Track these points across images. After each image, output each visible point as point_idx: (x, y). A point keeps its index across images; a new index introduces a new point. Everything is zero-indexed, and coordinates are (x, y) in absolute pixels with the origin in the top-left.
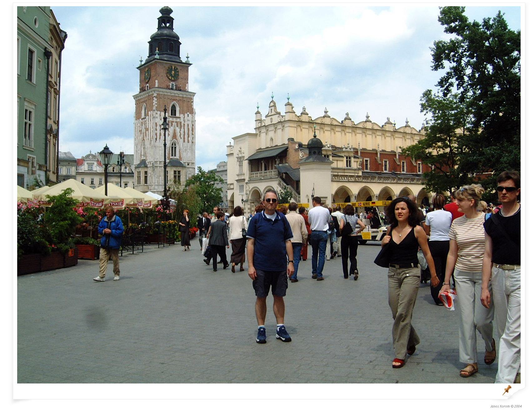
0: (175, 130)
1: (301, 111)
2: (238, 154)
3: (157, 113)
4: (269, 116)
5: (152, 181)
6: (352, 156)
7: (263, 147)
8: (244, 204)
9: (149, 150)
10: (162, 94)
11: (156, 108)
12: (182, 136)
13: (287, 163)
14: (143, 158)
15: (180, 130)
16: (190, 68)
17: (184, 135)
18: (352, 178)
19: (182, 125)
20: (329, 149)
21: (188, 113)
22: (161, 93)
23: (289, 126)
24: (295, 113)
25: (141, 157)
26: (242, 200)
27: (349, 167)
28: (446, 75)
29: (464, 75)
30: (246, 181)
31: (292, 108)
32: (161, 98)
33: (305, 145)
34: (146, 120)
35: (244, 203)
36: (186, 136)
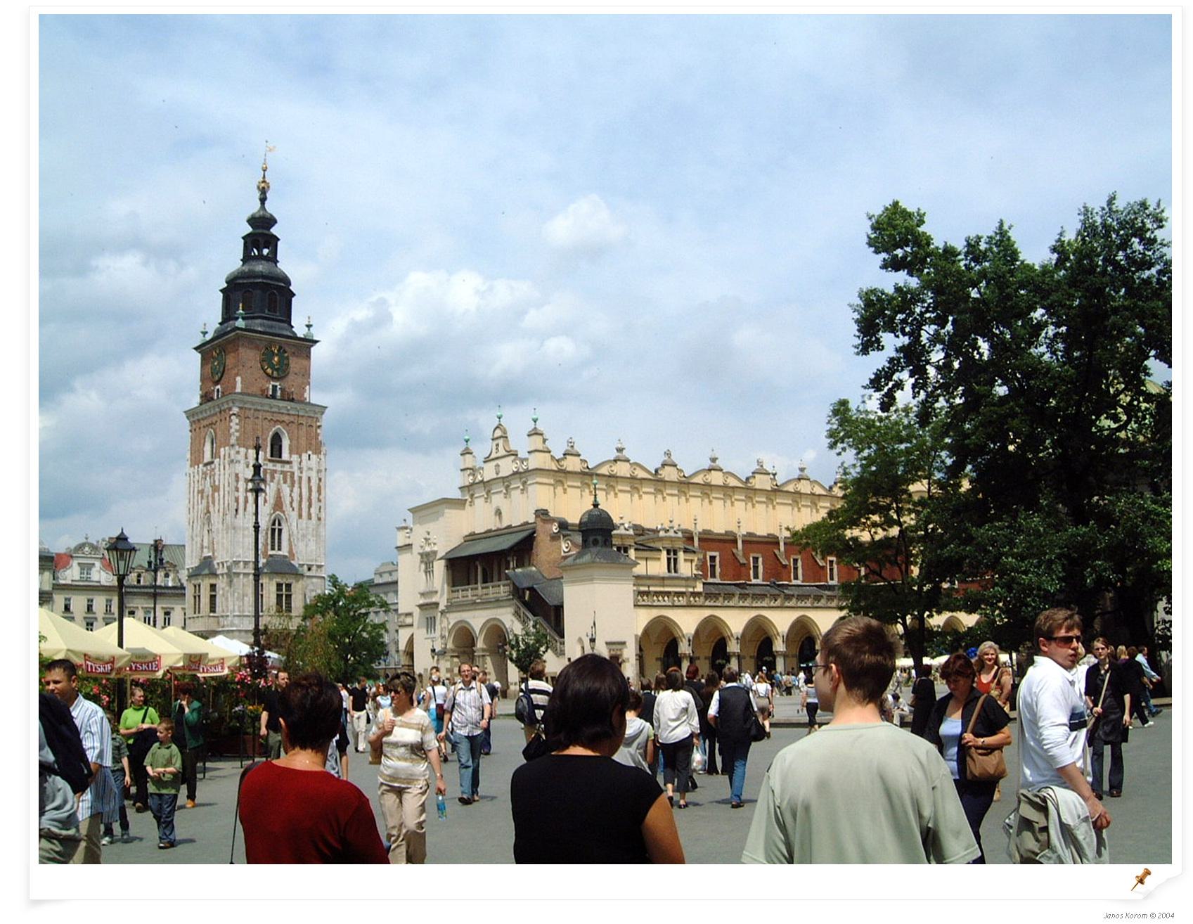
0: (279, 491)
1: (565, 447)
2: (422, 547)
3: (238, 452)
4: (493, 459)
5: (227, 607)
6: (680, 548)
7: (480, 529)
8: (438, 660)
9: (220, 537)
10: (250, 409)
11: (238, 439)
12: (295, 505)
13: (533, 565)
14: (207, 553)
15: (292, 491)
17: (300, 502)
18: (681, 599)
19: (296, 478)
20: (627, 532)
21: (310, 452)
23: (537, 483)
25: (202, 551)
26: (433, 651)
27: (673, 574)
28: (888, 365)
29: (928, 362)
30: (442, 607)
31: (544, 441)
32: (248, 418)
33: (573, 525)
34: (213, 466)
35: (436, 657)
36: (305, 505)
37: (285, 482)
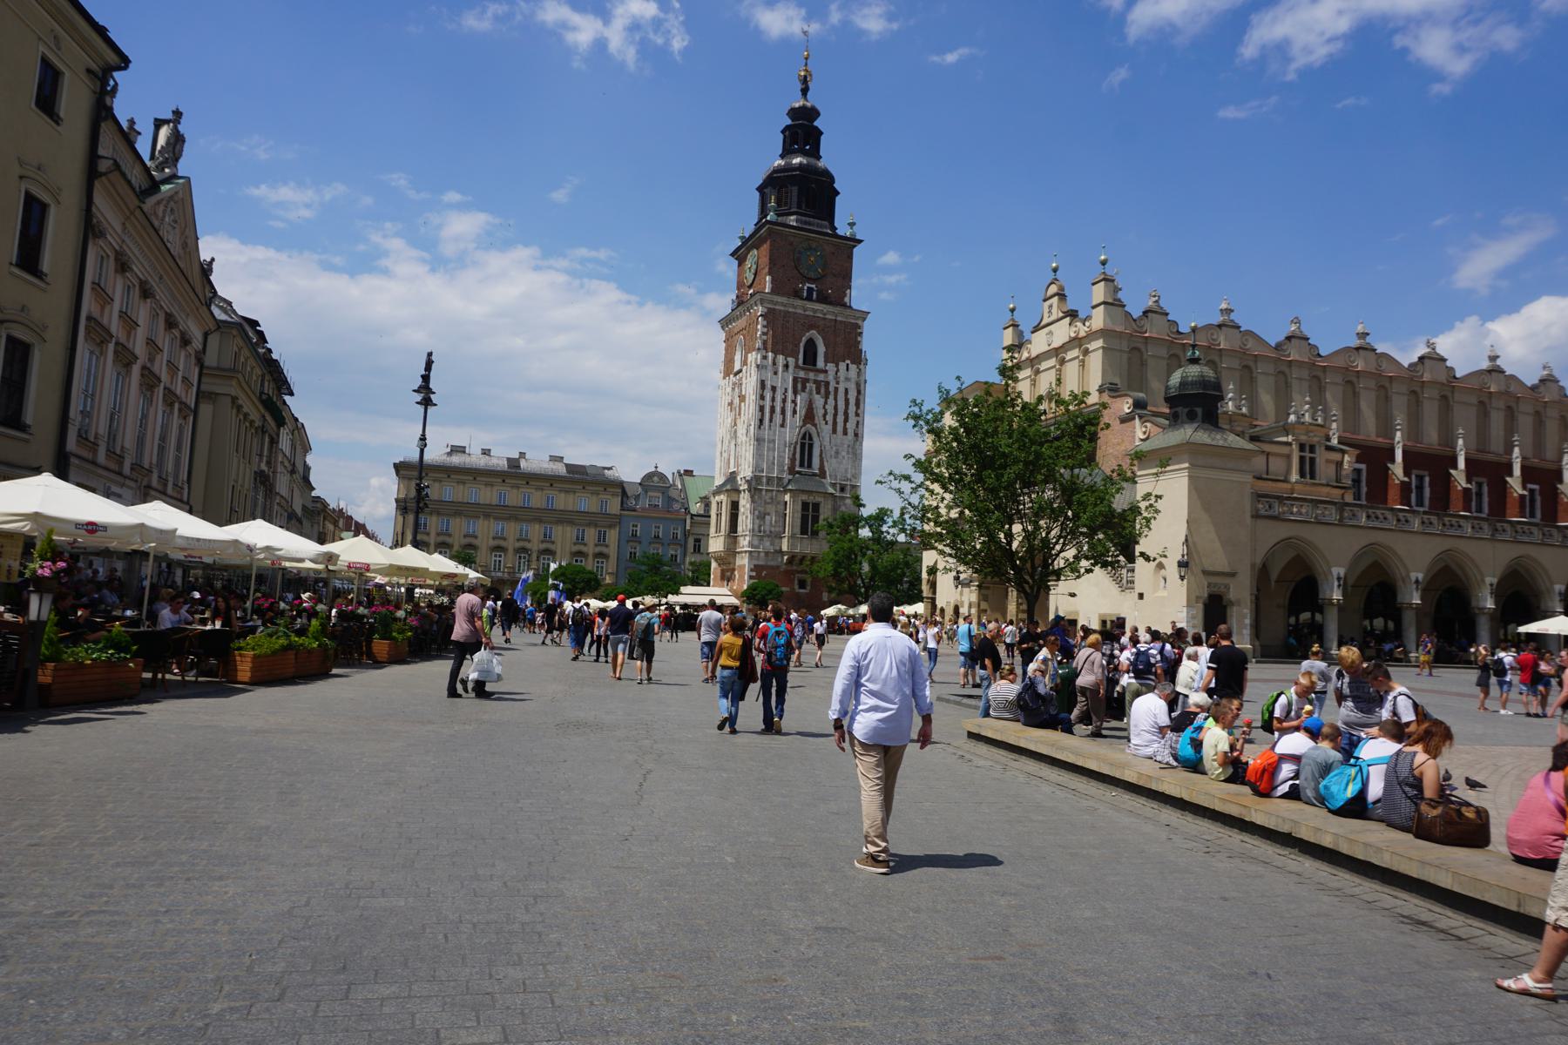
12: (829, 418)
15: (826, 403)
16: (858, 251)
17: (835, 415)
19: (831, 389)
21: (848, 362)
22: (777, 307)
24: (1124, 306)
36: (840, 419)
37: (818, 393)
